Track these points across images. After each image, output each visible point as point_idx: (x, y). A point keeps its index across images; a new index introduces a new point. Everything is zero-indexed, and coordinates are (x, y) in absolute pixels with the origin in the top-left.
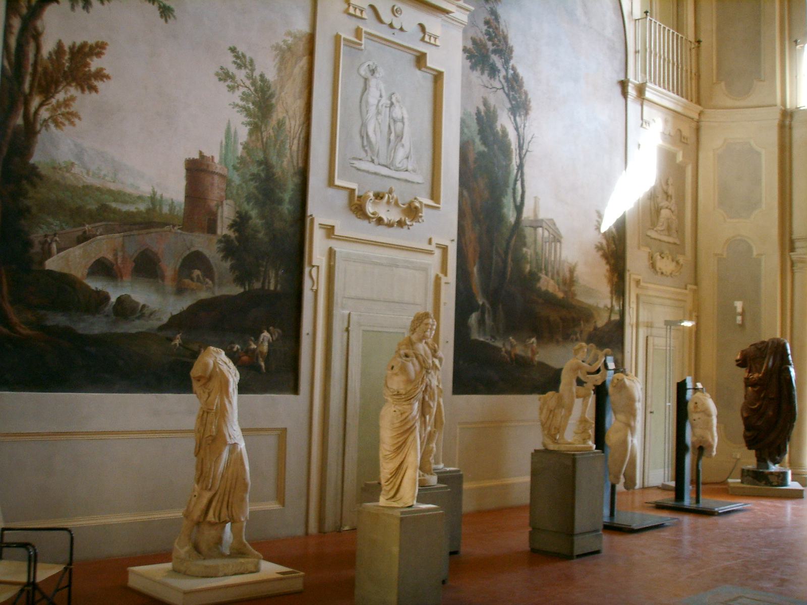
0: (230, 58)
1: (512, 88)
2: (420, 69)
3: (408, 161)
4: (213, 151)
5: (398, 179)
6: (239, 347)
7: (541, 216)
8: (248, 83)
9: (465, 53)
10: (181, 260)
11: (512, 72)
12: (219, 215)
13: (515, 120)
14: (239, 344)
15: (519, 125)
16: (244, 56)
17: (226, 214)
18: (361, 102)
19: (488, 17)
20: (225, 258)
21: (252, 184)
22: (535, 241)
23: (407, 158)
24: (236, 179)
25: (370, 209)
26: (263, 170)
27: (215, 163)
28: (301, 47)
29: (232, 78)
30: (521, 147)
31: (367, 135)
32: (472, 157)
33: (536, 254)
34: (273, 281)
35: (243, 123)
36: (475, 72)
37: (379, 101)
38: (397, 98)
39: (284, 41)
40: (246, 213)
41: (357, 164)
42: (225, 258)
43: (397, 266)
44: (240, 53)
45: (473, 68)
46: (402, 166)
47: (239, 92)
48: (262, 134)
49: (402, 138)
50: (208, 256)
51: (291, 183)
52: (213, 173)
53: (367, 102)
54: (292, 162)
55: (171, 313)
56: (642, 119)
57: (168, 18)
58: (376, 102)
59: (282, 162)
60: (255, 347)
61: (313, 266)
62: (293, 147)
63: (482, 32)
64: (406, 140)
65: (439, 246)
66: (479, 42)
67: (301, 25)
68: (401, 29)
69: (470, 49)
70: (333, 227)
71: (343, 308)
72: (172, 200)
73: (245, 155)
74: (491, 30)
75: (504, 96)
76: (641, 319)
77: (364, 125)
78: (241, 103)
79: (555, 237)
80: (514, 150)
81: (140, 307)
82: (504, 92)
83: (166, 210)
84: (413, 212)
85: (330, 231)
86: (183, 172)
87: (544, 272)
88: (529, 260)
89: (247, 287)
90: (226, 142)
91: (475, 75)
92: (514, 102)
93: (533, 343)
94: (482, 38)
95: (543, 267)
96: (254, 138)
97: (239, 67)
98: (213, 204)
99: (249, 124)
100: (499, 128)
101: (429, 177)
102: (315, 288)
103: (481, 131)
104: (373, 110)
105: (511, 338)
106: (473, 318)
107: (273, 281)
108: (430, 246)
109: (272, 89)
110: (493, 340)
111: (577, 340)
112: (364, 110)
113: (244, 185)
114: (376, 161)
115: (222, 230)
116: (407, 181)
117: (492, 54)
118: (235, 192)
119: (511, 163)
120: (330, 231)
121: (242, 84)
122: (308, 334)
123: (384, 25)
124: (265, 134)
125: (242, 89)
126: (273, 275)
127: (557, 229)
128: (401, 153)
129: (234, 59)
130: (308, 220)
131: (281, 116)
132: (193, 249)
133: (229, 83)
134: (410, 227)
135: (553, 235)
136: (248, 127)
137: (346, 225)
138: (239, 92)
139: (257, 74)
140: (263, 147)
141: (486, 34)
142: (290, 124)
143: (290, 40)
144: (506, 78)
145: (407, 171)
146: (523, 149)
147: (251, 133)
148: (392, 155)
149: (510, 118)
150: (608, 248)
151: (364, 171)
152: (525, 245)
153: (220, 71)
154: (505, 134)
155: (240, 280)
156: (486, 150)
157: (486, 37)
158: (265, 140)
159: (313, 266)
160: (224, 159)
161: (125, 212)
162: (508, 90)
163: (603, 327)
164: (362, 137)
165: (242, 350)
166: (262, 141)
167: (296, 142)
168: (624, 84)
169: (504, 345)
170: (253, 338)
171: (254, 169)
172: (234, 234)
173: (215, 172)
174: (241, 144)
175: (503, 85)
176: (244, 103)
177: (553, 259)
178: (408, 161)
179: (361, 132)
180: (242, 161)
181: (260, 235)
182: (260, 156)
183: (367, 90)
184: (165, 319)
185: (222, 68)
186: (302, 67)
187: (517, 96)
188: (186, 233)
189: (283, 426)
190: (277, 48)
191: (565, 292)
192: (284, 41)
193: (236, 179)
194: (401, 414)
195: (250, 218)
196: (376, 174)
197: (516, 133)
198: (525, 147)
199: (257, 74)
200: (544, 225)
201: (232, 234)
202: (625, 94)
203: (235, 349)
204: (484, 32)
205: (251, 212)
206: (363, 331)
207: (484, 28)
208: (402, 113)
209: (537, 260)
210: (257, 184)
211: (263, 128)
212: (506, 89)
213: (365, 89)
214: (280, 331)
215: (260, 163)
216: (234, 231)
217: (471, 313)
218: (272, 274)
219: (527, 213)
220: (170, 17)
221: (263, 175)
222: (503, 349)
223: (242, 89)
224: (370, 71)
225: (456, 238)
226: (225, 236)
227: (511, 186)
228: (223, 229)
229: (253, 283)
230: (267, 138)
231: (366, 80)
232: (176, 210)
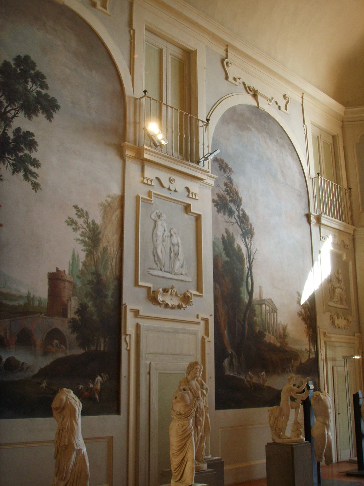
0: (74, 211)
1: (242, 222)
2: (187, 214)
3: (182, 269)
4: (65, 268)
5: (177, 280)
6: (82, 387)
7: (264, 297)
8: (85, 226)
9: (213, 203)
10: (45, 335)
11: (242, 213)
12: (69, 306)
13: (245, 241)
14: (82, 385)
15: (248, 244)
16: (82, 210)
17: (73, 305)
18: (153, 235)
19: (226, 181)
20: (73, 332)
21: (89, 286)
22: (261, 313)
23: (182, 267)
24: (79, 284)
25: (160, 298)
26: (95, 278)
27: (66, 274)
28: (116, 204)
29: (76, 223)
30: (249, 257)
31: (157, 255)
32: (220, 265)
33: (262, 320)
34: (102, 345)
35: (82, 250)
36: (220, 214)
37: (163, 234)
38: (174, 231)
40: (85, 304)
41: (152, 272)
42: (73, 332)
43: (178, 333)
44: (80, 209)
45: (219, 211)
46: (179, 272)
47: (79, 232)
48: (94, 257)
49: (178, 255)
50: (62, 331)
51: (112, 285)
52: (65, 281)
53: (156, 234)
54: (113, 272)
55: (40, 367)
56: (320, 236)
57: (37, 190)
58: (162, 235)
59: (107, 272)
60: (93, 386)
61: (127, 335)
62: (113, 263)
63: (223, 190)
64: (181, 256)
65: (203, 319)
66: (221, 196)
67: (116, 191)
68: (175, 191)
70: (138, 311)
71: (146, 360)
72: (40, 298)
73: (84, 269)
74: (228, 189)
75: (238, 227)
76: (328, 356)
77: (155, 249)
79: (273, 310)
80: (246, 259)
81: (21, 364)
82: (238, 225)
83: (36, 304)
84: (186, 299)
85: (136, 313)
86: (47, 280)
87: (267, 331)
88: (258, 325)
89: (87, 349)
90: (72, 262)
91: (220, 215)
92: (244, 231)
93: (263, 375)
94: (223, 193)
95: (267, 329)
96: (89, 259)
97: (79, 217)
98: (65, 299)
99: (86, 250)
100: (236, 246)
101: (196, 278)
102: (128, 348)
103: (225, 249)
104: (160, 239)
105: (249, 373)
106: (226, 362)
107: (102, 345)
108: (198, 319)
109: (100, 229)
110: (239, 375)
111: (290, 371)
112: (155, 240)
113: (84, 287)
114: (163, 269)
115: (71, 315)
116: (182, 281)
117: (230, 202)
118: (78, 291)
119: (244, 267)
120: (136, 313)
121: (81, 227)
122: (125, 377)
123: (165, 189)
124: (95, 256)
125: (82, 230)
126: (103, 341)
127: (274, 304)
128: (178, 264)
129: (76, 212)
130: (123, 307)
131: (105, 245)
132: (53, 327)
133: (74, 226)
134: (185, 309)
135: (271, 308)
136: (86, 252)
137: (146, 309)
138: (79, 232)
139: (90, 221)
140: (95, 264)
142: (111, 249)
143: (109, 200)
144: (238, 216)
145: (182, 274)
146: (251, 258)
147: (87, 256)
148: (173, 266)
149: (242, 240)
150: (305, 314)
151: (156, 276)
152: (255, 315)
153: (68, 220)
154: (240, 249)
155: (82, 345)
156: (229, 259)
157: (226, 193)
158: (96, 260)
159: (127, 335)
160: (71, 272)
161: (12, 306)
162: (240, 223)
163: (305, 362)
164: (154, 256)
165: (84, 388)
166: (94, 261)
167: (114, 260)
168: (308, 216)
169: (245, 377)
170: (91, 381)
171: (90, 277)
172: (78, 317)
173: (66, 280)
174: (81, 262)
176: (83, 238)
177: (272, 323)
178: (182, 269)
179: (153, 252)
180: (82, 272)
181: (95, 317)
182: (93, 269)
183: (156, 228)
184: (36, 372)
185: (69, 218)
186: (117, 216)
187: (246, 226)
188: (49, 317)
189: (110, 435)
190: (102, 205)
191: (281, 343)
192: (106, 200)
193: (79, 284)
194: (183, 427)
195: (88, 307)
196: (163, 277)
197: (246, 249)
198: (252, 256)
199: (90, 221)
200: (266, 303)
201: (77, 317)
202: (309, 221)
203: (80, 388)
204: (224, 190)
205: (88, 304)
206: (159, 373)
207: (224, 188)
208: (177, 240)
209: (263, 324)
210: (91, 286)
211: (95, 253)
212: (239, 223)
213: (155, 227)
214: (107, 375)
215: (93, 274)
216: (78, 316)
217: (224, 359)
218: (102, 341)
219: (255, 296)
220: (38, 189)
221: (95, 281)
222: (245, 380)
223: (82, 230)
224: (158, 216)
225: (213, 314)
226: (73, 319)
227: (245, 280)
228: (71, 314)
229: (91, 347)
230: (97, 258)
232: (43, 304)
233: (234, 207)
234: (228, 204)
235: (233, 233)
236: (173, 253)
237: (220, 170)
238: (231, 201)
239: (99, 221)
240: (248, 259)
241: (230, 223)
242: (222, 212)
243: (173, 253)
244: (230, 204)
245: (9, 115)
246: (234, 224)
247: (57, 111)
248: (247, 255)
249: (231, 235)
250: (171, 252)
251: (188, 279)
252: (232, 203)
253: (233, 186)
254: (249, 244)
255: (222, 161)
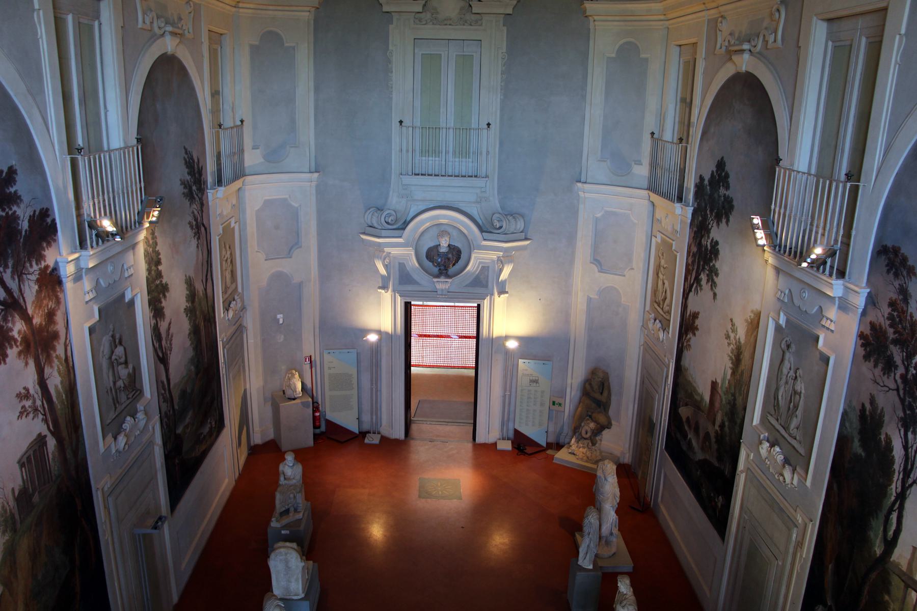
4: (719, 381)
5: (789, 443)
9: (860, 339)
15: (910, 445)
16: (735, 325)
18: (778, 370)
31: (778, 399)
36: (867, 363)
37: (789, 373)
39: (750, 316)
41: (770, 418)
52: (718, 392)
58: (786, 373)
63: (883, 316)
64: (799, 412)
66: (878, 327)
69: (867, 335)
74: (895, 314)
75: (897, 400)
77: (777, 389)
78: (731, 355)
82: (899, 395)
92: (908, 412)
94: (883, 324)
103: (862, 432)
112: (779, 379)
116: (794, 447)
117: (891, 344)
119: (890, 485)
124: (736, 377)
128: (794, 423)
133: (728, 341)
139: (737, 337)
141: (888, 319)
144: (904, 377)
145: (795, 439)
146: (909, 477)
149: (900, 430)
154: (889, 448)
156: (863, 454)
157: (888, 322)
162: (904, 394)
175: (898, 386)
195: (725, 426)
197: (903, 452)
199: (737, 337)
204: (886, 315)
207: (887, 310)
212: (901, 392)
227: (885, 511)
231: (784, 352)
233: (897, 355)
234: (887, 348)
235: (883, 408)
236: (792, 404)
237: (888, 272)
238: (895, 342)
239: (742, 341)
240: (901, 476)
241: (881, 386)
242: (872, 360)
243: (792, 404)
244: (892, 347)
245: (710, 226)
246: (891, 391)
247: (732, 213)
248: (902, 465)
249: (879, 411)
250: (791, 402)
251: (802, 451)
252: (896, 345)
253: (908, 307)
254: (912, 447)
255: (896, 251)
